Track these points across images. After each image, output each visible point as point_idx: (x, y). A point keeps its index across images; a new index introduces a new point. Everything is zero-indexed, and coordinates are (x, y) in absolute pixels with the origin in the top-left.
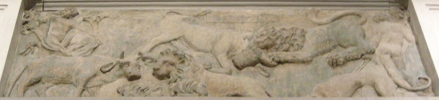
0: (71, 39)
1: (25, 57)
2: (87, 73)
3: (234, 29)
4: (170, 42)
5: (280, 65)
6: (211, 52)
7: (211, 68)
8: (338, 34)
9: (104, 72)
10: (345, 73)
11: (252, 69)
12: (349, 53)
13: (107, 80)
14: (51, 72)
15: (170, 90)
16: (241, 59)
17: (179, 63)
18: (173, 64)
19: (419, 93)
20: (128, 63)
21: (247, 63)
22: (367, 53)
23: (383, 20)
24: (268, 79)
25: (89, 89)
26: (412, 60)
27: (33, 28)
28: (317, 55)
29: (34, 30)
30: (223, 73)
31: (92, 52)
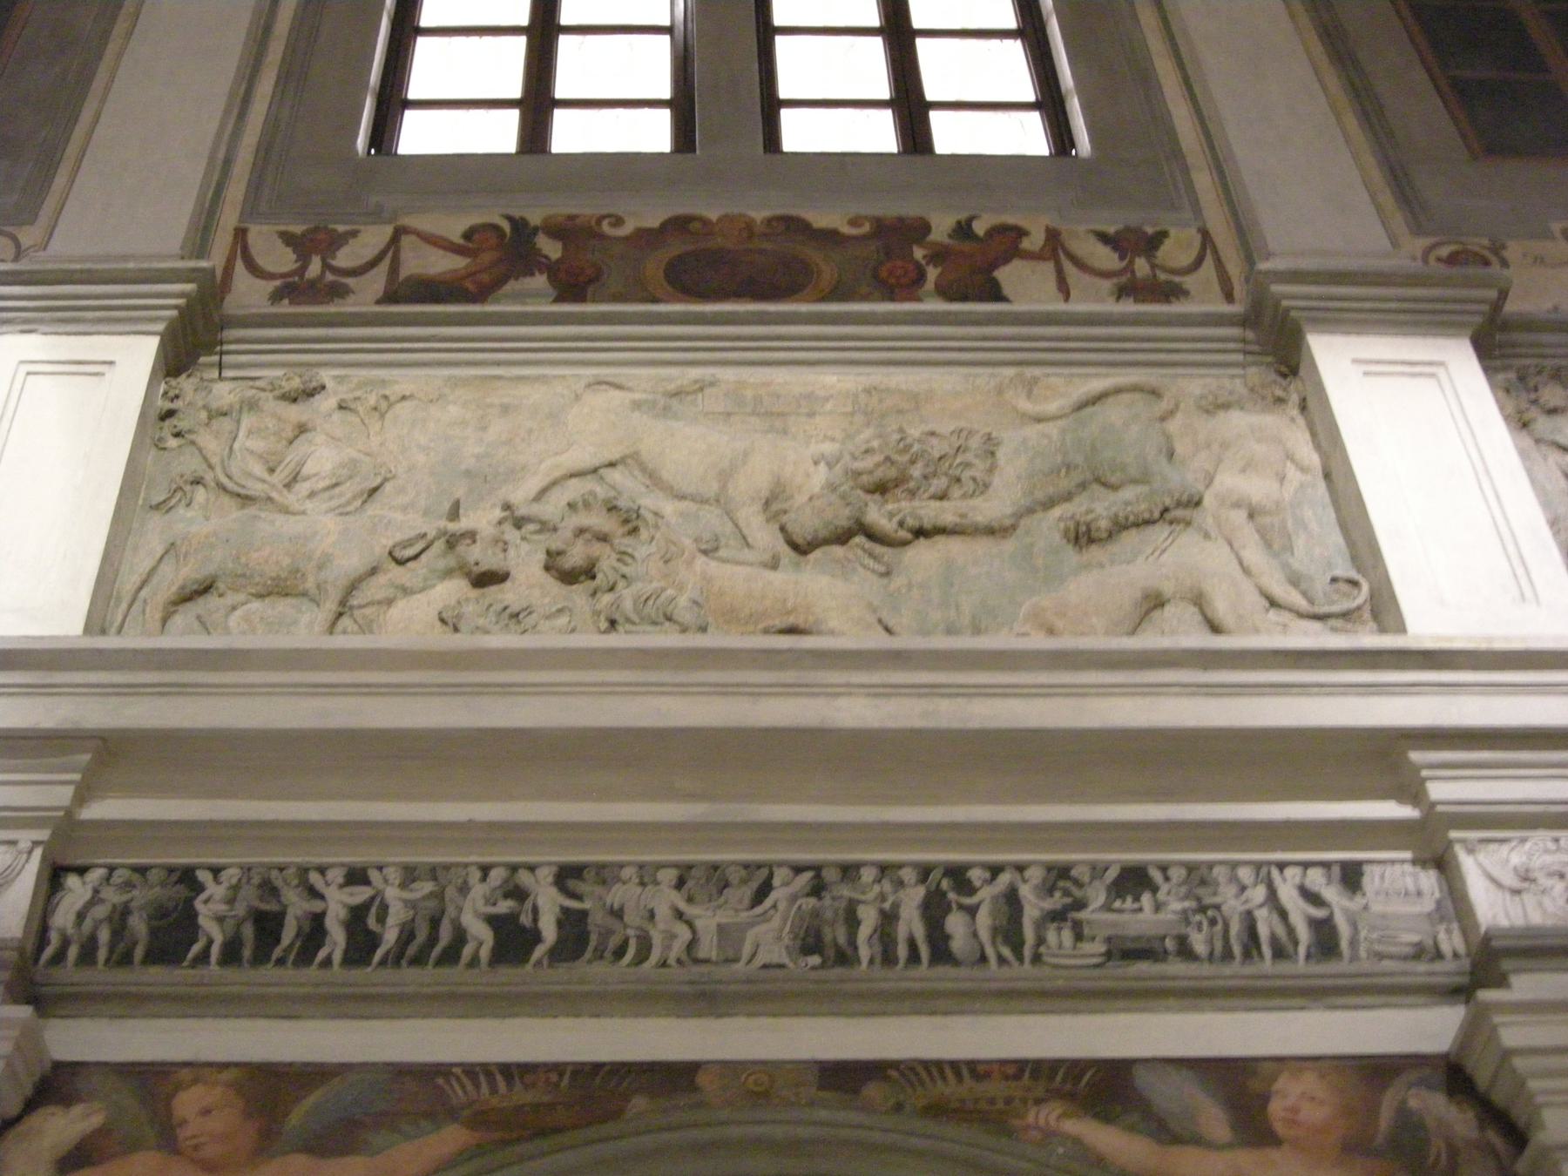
0: (302, 464)
1: (167, 517)
2: (350, 563)
3: (785, 432)
4: (595, 471)
5: (922, 539)
6: (718, 501)
7: (716, 549)
8: (1093, 448)
10: (1112, 562)
11: (838, 551)
12: (1127, 503)
13: (408, 584)
14: (243, 560)
15: (597, 613)
16: (806, 523)
17: (623, 535)
18: (603, 538)
19: (1333, 622)
20: (471, 535)
21: (823, 533)
22: (1179, 504)
23: (1226, 406)
24: (885, 581)
25: (357, 613)
26: (1313, 526)
27: (190, 431)
28: (1030, 511)
30: (752, 564)
31: (365, 502)
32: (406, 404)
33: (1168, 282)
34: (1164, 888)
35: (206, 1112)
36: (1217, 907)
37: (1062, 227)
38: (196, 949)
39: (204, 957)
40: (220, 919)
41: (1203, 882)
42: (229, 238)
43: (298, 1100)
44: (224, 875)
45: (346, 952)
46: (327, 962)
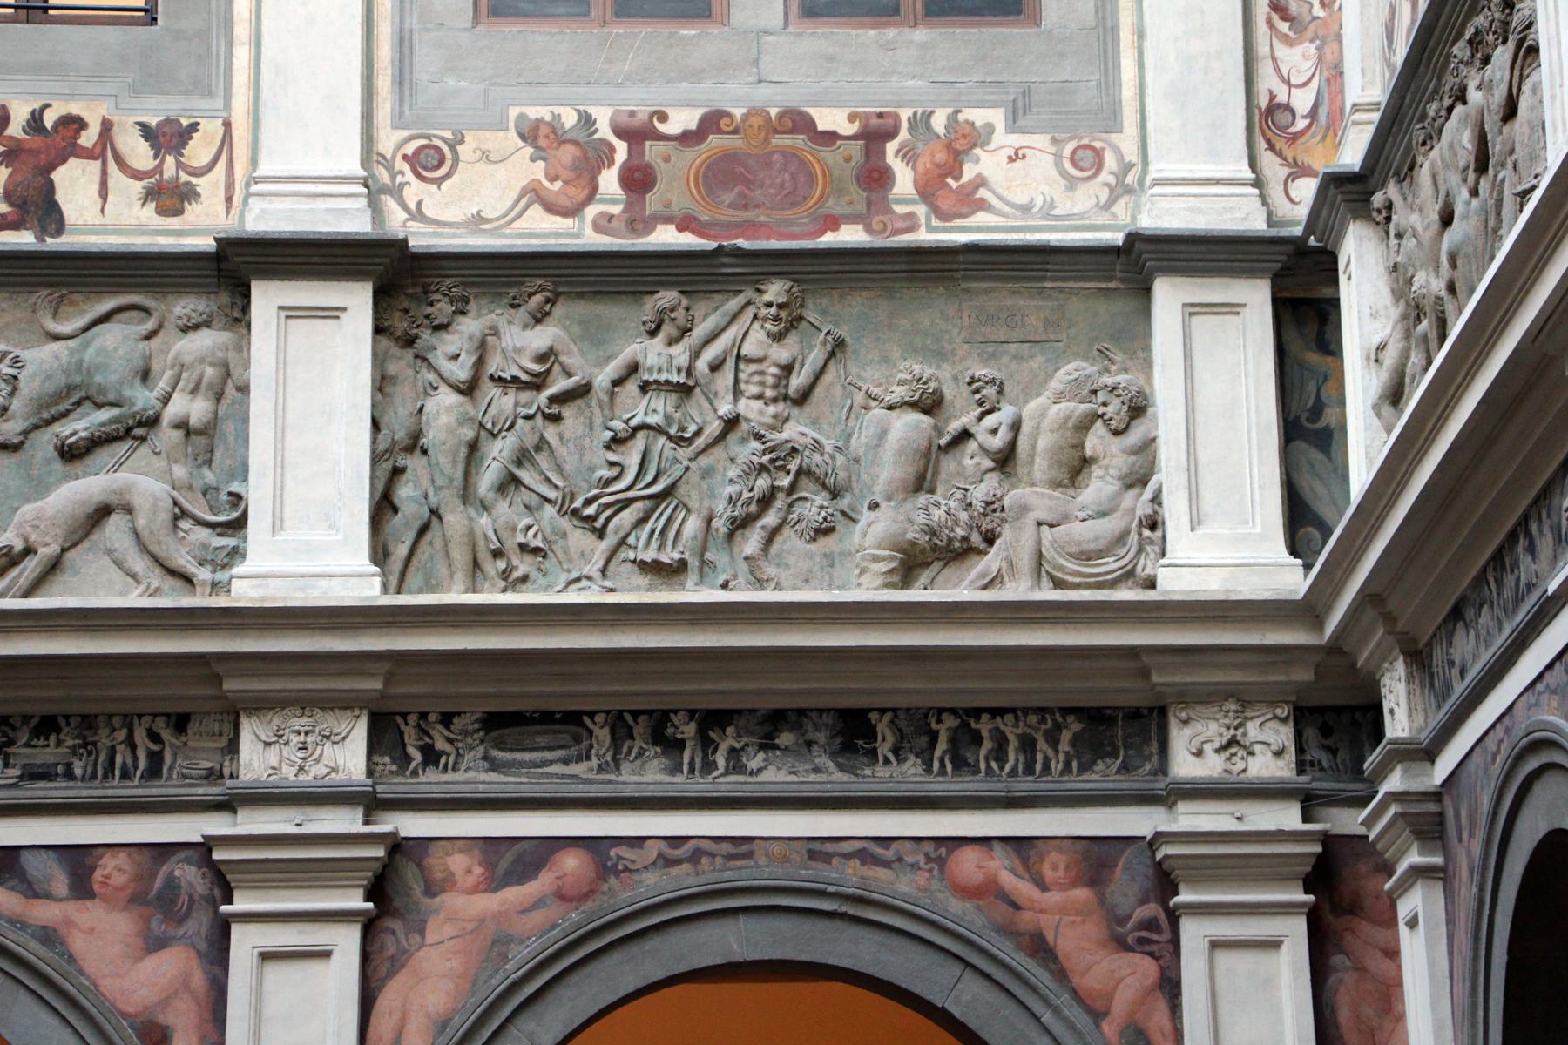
19: (219, 530)
22: (140, 424)
28: (36, 427)
33: (188, 183)
34: (66, 730)
36: (94, 744)
37: (115, 119)
41: (90, 727)
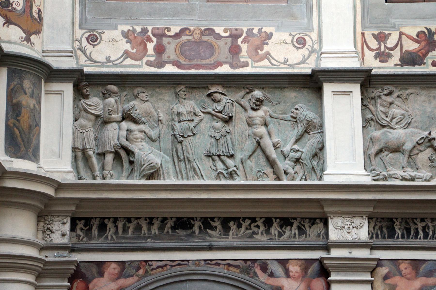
9: (419, 144)
25: (412, 157)
27: (367, 105)
29: (368, 106)
32: (412, 95)
35: (406, 269)
38: (396, 235)
39: (398, 237)
40: (399, 229)
42: (361, 36)
43: (421, 267)
44: (398, 220)
45: (423, 236)
46: (420, 238)
